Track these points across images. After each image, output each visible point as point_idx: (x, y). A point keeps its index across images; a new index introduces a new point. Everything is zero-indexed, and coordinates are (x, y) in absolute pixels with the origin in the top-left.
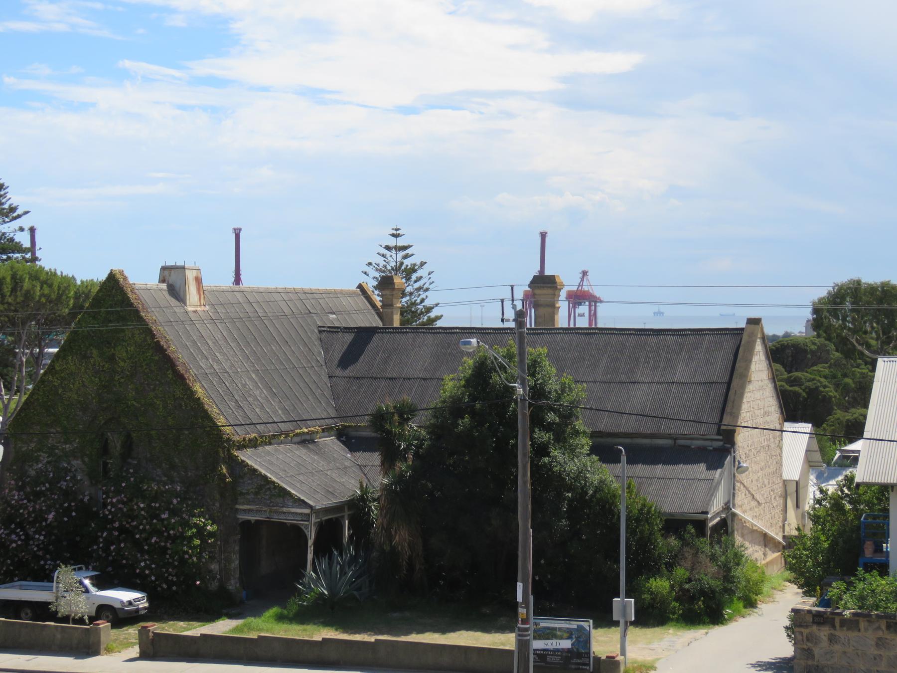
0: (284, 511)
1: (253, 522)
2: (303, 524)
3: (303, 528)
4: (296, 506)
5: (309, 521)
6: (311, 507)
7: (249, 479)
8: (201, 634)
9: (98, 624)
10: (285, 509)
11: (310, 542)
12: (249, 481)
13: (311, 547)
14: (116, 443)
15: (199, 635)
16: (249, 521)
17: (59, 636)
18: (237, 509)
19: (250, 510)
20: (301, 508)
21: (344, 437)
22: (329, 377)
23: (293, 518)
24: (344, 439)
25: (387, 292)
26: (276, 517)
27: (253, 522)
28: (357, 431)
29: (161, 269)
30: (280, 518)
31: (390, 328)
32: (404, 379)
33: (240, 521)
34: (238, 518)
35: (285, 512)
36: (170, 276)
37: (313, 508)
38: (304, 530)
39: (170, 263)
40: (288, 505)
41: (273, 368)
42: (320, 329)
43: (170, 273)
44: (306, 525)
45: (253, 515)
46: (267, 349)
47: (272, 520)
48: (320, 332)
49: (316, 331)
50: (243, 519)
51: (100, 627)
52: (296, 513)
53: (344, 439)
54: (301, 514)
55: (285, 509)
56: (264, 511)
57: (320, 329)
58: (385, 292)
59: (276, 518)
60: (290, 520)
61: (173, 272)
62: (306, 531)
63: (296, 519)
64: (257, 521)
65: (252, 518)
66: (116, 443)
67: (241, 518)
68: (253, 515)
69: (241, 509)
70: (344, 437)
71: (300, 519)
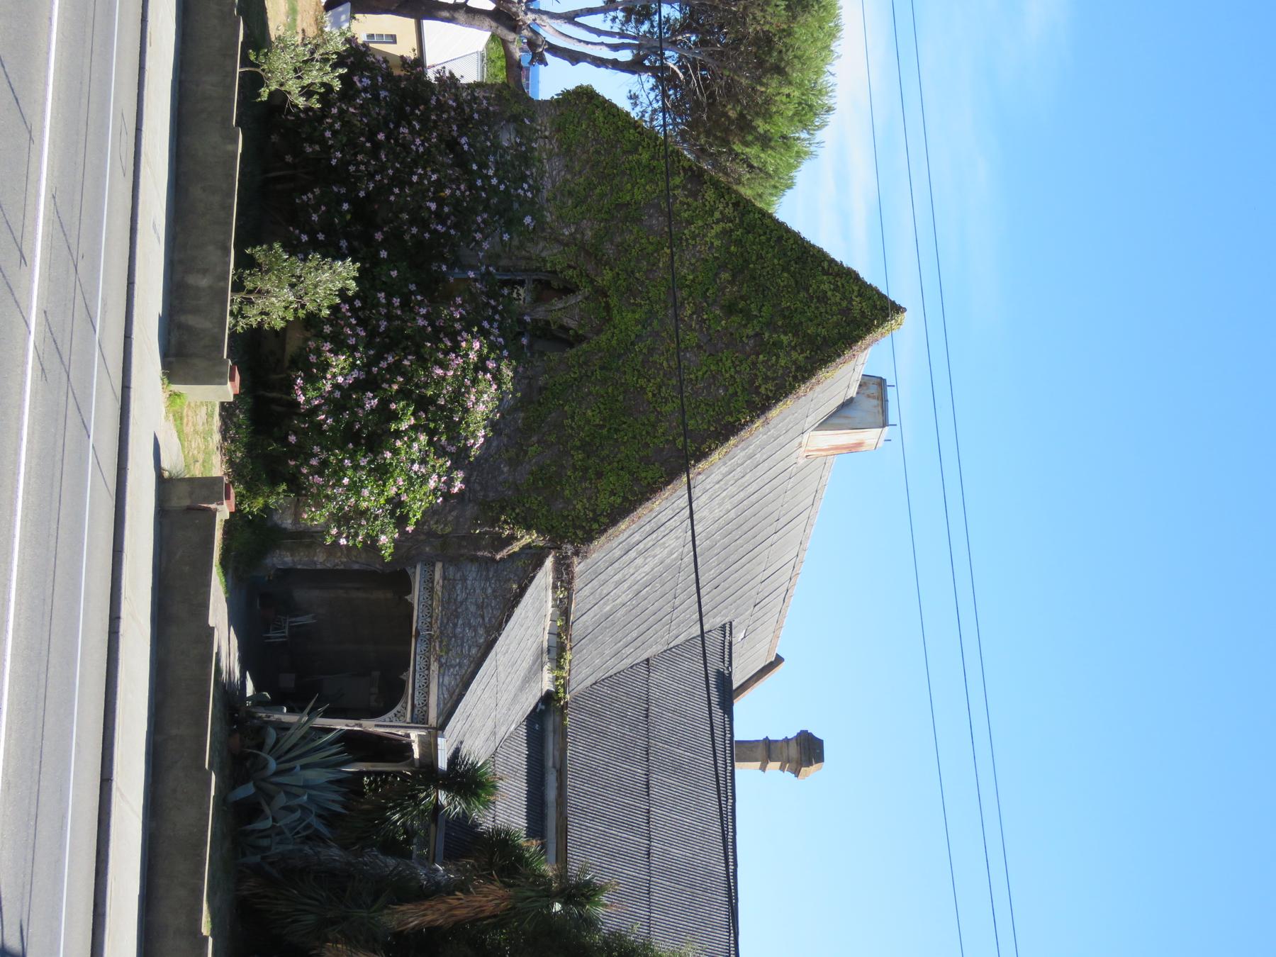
0: (432, 668)
1: (408, 597)
2: (406, 708)
3: (398, 707)
4: (443, 694)
5: (412, 722)
6: (442, 727)
7: (494, 591)
8: (213, 629)
9: (232, 379)
10: (434, 667)
11: (370, 726)
12: (489, 591)
13: (360, 726)
14: (562, 311)
15: (211, 623)
16: (409, 590)
17: (204, 282)
18: (434, 565)
19: (431, 590)
20: (438, 705)
21: (543, 707)
22: (648, 660)
23: (417, 686)
24: (541, 707)
25: (793, 751)
26: (418, 651)
27: (408, 597)
28: (554, 732)
29: (881, 378)
30: (418, 658)
31: (732, 757)
32: (649, 811)
33: (410, 572)
34: (415, 567)
35: (428, 669)
36: (869, 396)
37: (440, 732)
38: (394, 711)
39: (891, 393)
40: (444, 675)
41: (680, 579)
42: (728, 626)
43: (874, 397)
44: (404, 716)
45: (421, 599)
46: (714, 562)
47: (413, 640)
48: (723, 627)
49: (727, 620)
50: (414, 577)
51: (226, 384)
52: (428, 693)
53: (541, 707)
54: (427, 705)
55: (434, 667)
56: (430, 623)
57: (728, 626)
58: (793, 746)
59: (417, 648)
60: (412, 678)
61: (875, 402)
62: (391, 714)
63: (417, 693)
64: (410, 607)
65: (416, 597)
66: (562, 311)
67: (415, 573)
68: (421, 599)
69: (433, 571)
70: (543, 707)
71: (416, 702)
